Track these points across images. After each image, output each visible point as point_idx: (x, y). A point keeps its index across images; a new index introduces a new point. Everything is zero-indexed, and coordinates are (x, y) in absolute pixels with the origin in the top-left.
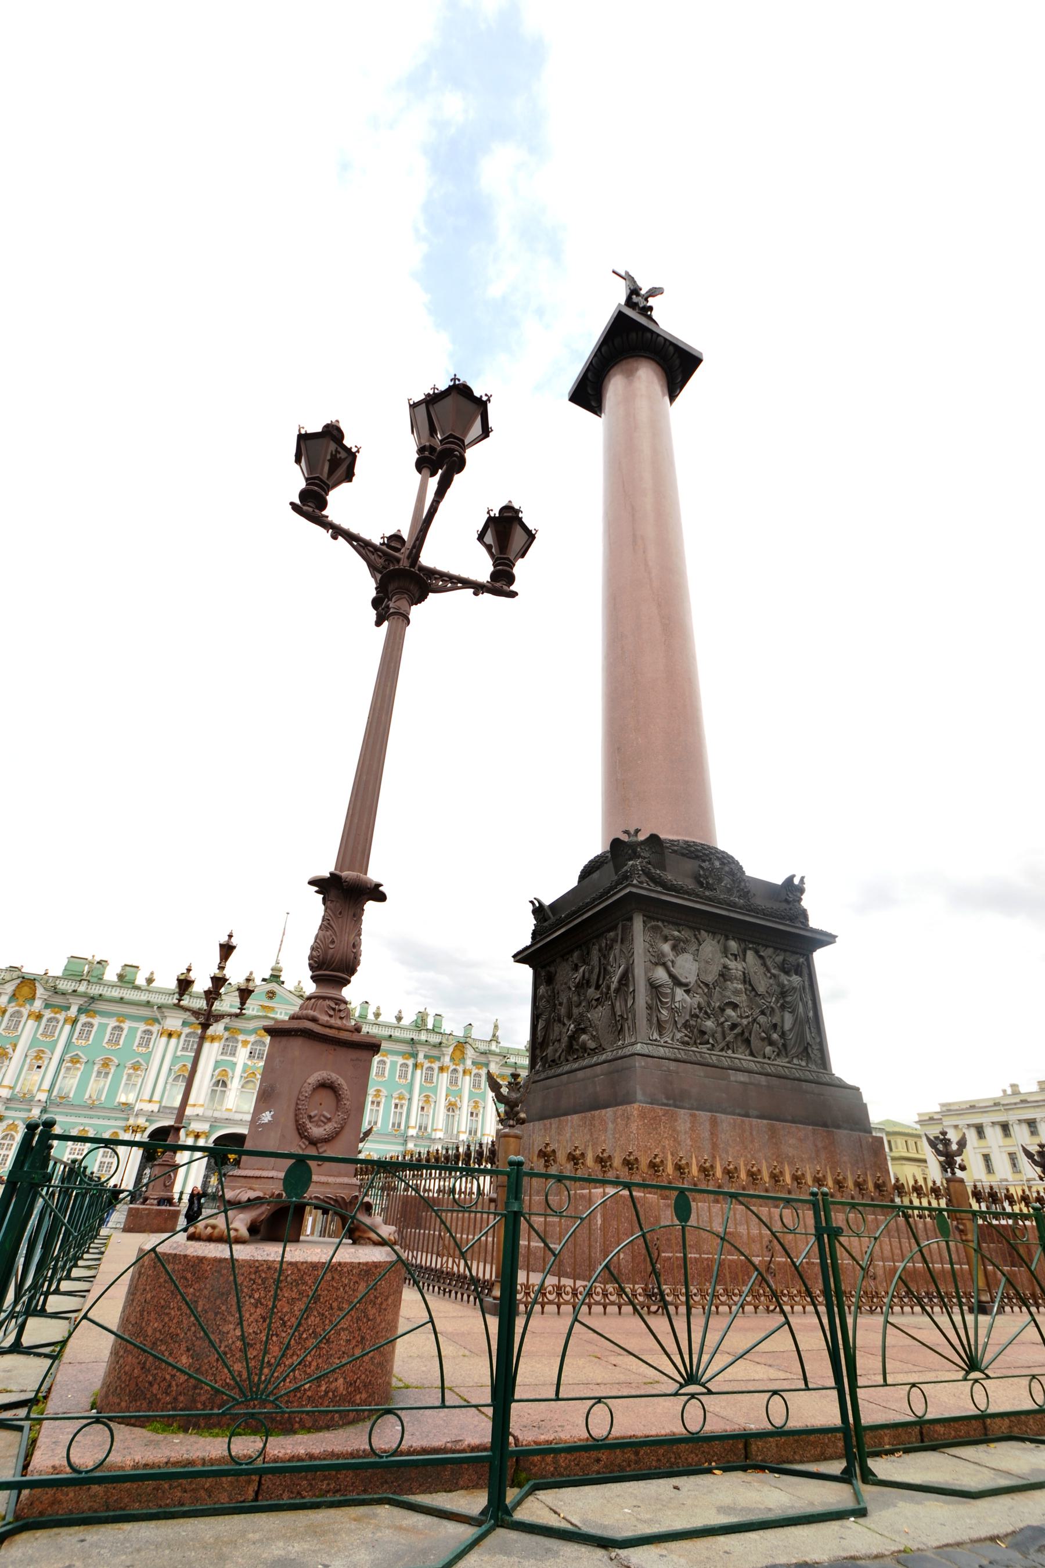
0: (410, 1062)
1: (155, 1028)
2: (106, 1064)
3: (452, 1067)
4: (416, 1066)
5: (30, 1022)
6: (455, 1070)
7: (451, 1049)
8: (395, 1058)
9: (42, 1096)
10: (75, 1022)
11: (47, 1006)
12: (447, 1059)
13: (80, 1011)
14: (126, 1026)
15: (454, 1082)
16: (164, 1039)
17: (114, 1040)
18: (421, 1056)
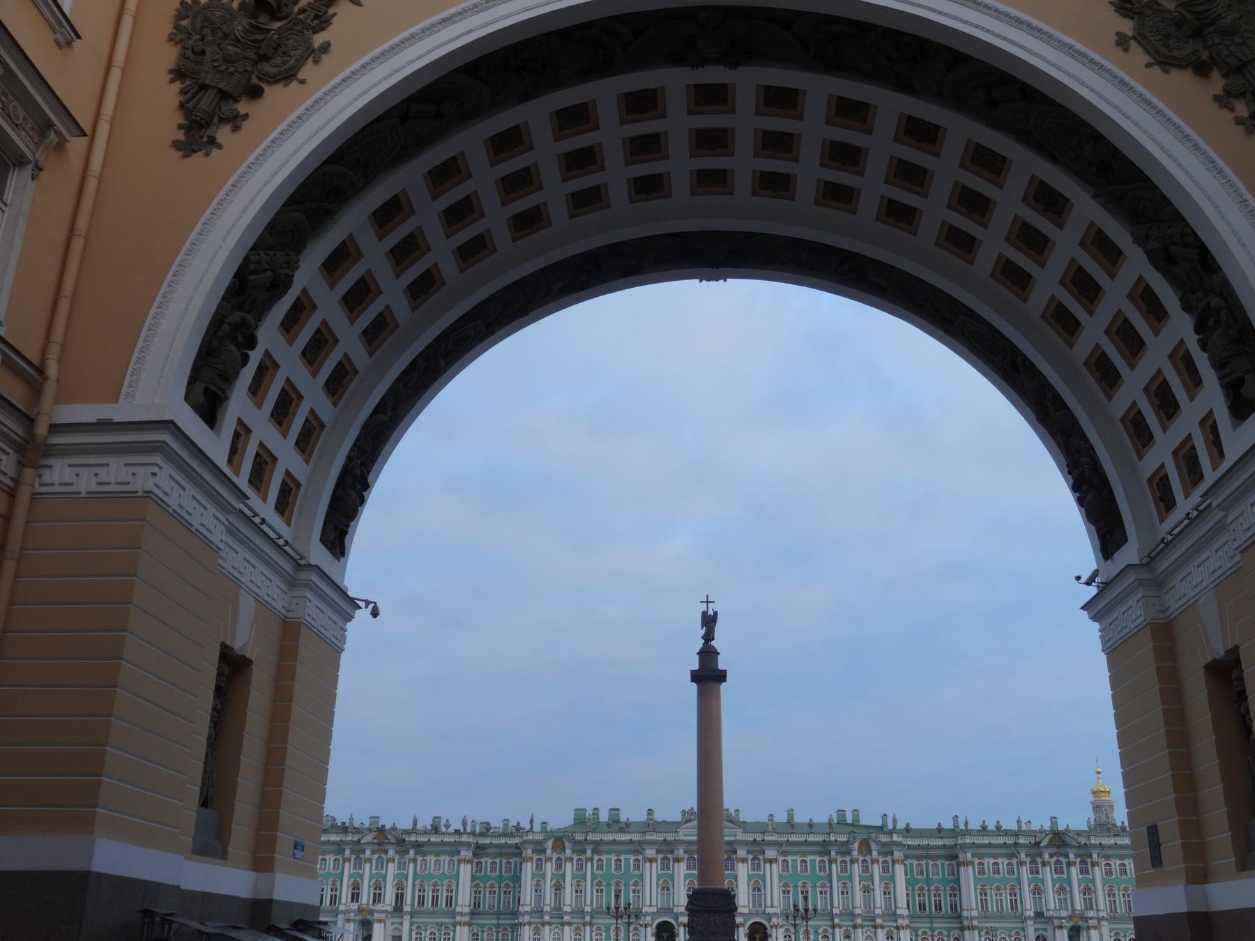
0: (826, 859)
1: (640, 857)
2: (618, 884)
3: (861, 859)
4: (831, 862)
5: (569, 865)
6: (864, 861)
7: (856, 845)
8: (812, 857)
9: (588, 909)
10: (592, 860)
11: (574, 852)
12: (855, 853)
13: (593, 852)
14: (622, 858)
15: (866, 869)
16: (648, 864)
17: (618, 868)
18: (833, 853)
